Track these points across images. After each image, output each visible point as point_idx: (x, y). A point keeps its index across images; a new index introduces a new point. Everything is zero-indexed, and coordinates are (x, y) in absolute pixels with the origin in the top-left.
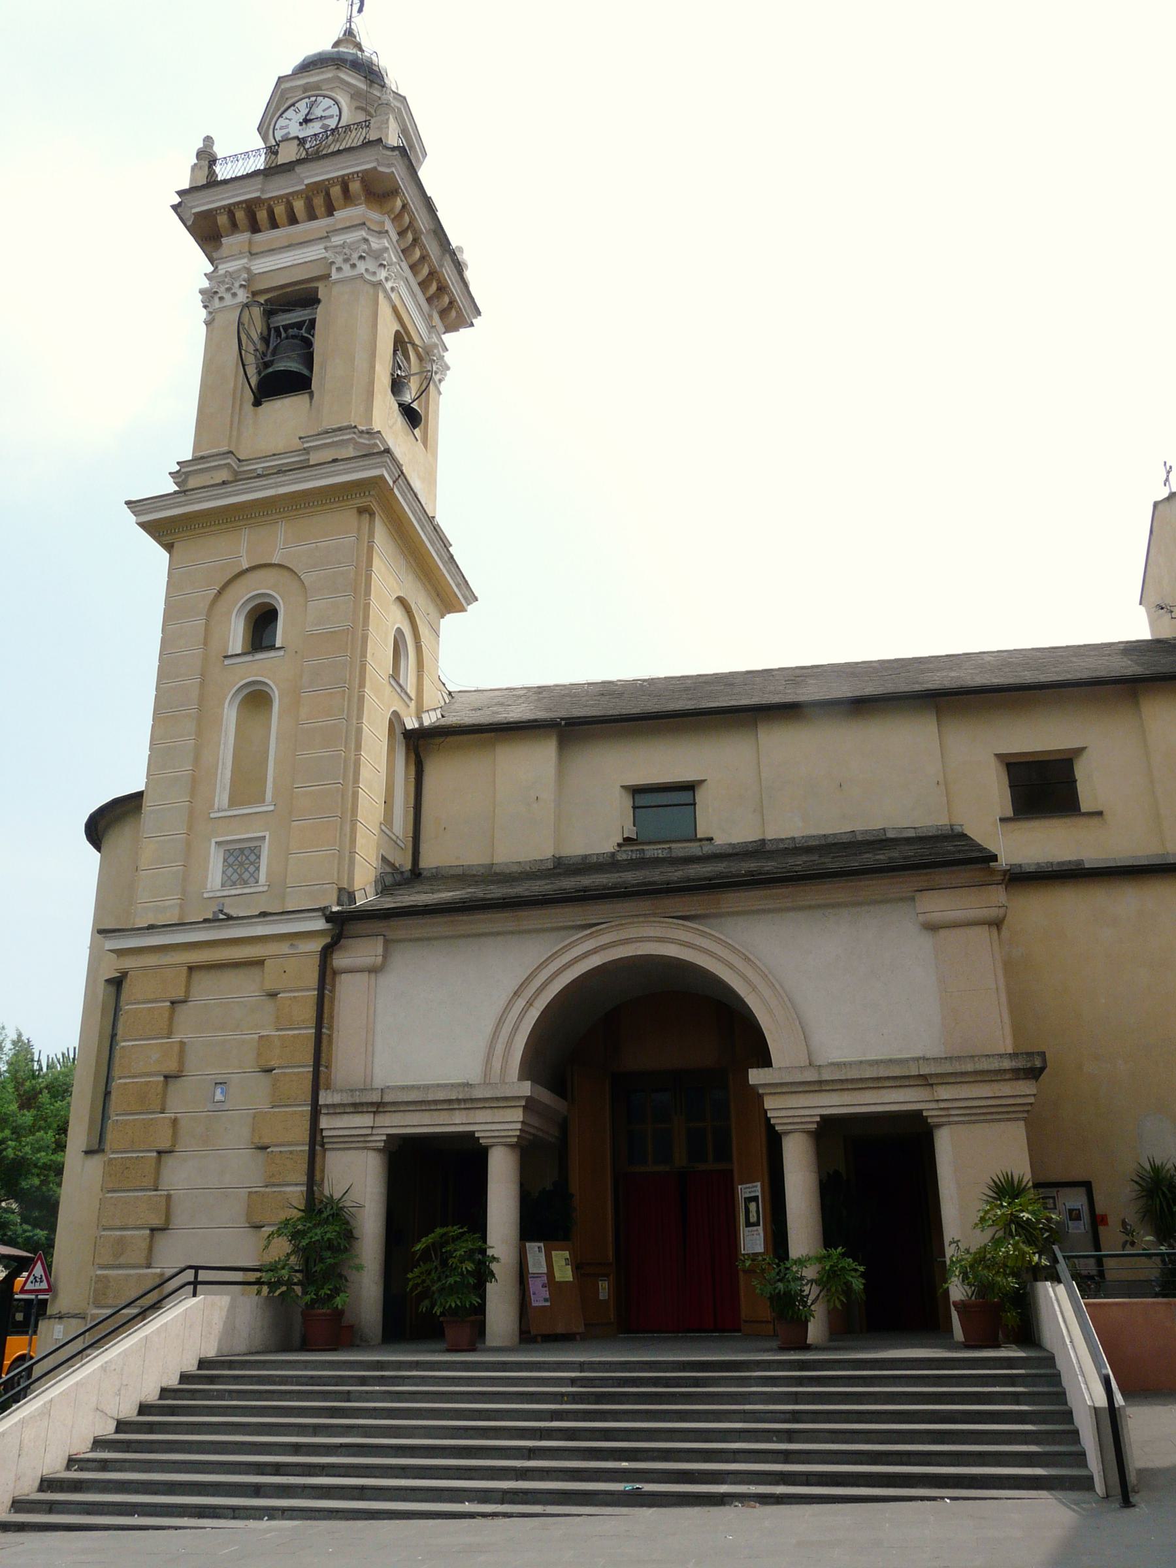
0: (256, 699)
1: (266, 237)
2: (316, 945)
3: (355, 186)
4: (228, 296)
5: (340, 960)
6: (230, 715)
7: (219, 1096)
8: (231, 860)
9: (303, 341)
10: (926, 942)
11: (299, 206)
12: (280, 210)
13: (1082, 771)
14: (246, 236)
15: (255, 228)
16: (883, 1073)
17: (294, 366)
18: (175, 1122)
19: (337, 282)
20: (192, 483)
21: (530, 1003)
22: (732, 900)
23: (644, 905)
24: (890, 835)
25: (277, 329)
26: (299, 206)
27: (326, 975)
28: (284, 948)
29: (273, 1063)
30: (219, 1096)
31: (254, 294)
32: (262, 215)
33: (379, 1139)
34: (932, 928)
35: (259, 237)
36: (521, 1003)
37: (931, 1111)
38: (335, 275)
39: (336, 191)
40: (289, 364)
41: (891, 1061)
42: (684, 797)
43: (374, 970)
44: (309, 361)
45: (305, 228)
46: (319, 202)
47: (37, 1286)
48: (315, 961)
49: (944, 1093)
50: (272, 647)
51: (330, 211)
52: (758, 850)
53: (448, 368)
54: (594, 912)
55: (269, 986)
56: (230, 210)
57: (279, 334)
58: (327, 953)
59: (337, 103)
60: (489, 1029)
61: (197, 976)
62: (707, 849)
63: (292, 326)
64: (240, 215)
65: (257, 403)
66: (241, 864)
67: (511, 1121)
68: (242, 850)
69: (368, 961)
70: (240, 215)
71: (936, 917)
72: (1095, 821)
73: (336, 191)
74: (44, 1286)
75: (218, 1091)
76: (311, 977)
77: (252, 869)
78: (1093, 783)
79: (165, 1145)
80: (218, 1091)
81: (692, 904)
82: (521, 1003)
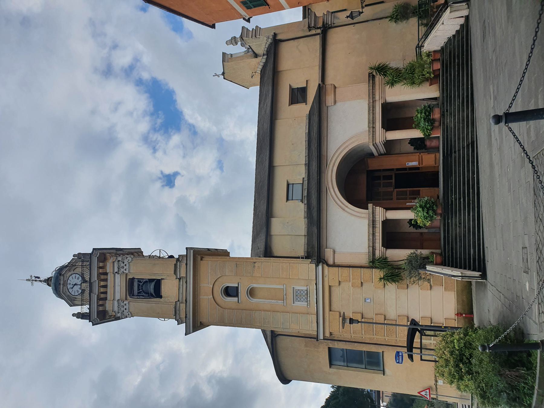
0: (251, 292)
1: (109, 296)
2: (326, 267)
3: (101, 264)
4: (125, 307)
5: (331, 262)
6: (254, 300)
7: (369, 301)
8: (299, 299)
9: (143, 283)
10: (338, 104)
11: (102, 283)
12: (102, 290)
13: (295, 86)
14: (107, 301)
15: (106, 299)
16: (371, 111)
17: (152, 285)
18: (376, 314)
19: (129, 271)
20: (183, 315)
21: (347, 207)
22: (324, 152)
23: (323, 175)
24: (307, 131)
25: (138, 293)
26: (102, 283)
27: (334, 265)
28: (326, 279)
29: (360, 282)
30: (369, 301)
31: (126, 299)
32: (102, 296)
33: (383, 249)
34: (335, 102)
35: (108, 298)
36: (346, 209)
37: (381, 101)
38: (127, 272)
39: (101, 271)
40: (151, 288)
41: (369, 111)
42: (291, 186)
43: (334, 252)
44: (151, 281)
45: (110, 283)
46: (102, 277)
47: (428, 394)
48: (331, 268)
49: (377, 98)
50: (237, 288)
51: (106, 274)
52: (308, 165)
53: (257, 27)
54: (324, 190)
55: (337, 284)
56: (99, 305)
57: (140, 293)
58: (328, 265)
59: (72, 275)
60: (353, 218)
61: (333, 309)
62: (306, 179)
63: (138, 287)
64: (101, 303)
65: (161, 297)
66: (300, 296)
67: (379, 211)
68: (296, 296)
69: (332, 253)
70: (101, 303)
71: (333, 101)
72: (309, 82)
73: (101, 271)
74: (428, 391)
75: (368, 301)
76: (336, 269)
77: (302, 292)
78: (299, 84)
79: (383, 317)
80: (368, 301)
81: (324, 162)
82: (346, 209)
